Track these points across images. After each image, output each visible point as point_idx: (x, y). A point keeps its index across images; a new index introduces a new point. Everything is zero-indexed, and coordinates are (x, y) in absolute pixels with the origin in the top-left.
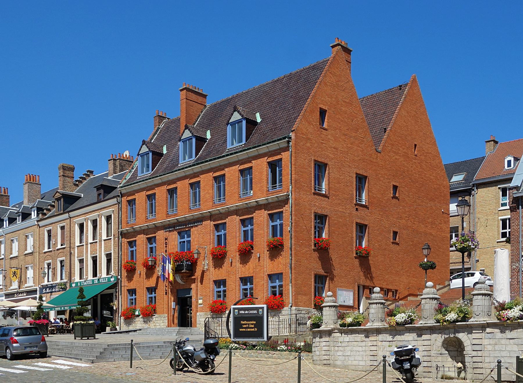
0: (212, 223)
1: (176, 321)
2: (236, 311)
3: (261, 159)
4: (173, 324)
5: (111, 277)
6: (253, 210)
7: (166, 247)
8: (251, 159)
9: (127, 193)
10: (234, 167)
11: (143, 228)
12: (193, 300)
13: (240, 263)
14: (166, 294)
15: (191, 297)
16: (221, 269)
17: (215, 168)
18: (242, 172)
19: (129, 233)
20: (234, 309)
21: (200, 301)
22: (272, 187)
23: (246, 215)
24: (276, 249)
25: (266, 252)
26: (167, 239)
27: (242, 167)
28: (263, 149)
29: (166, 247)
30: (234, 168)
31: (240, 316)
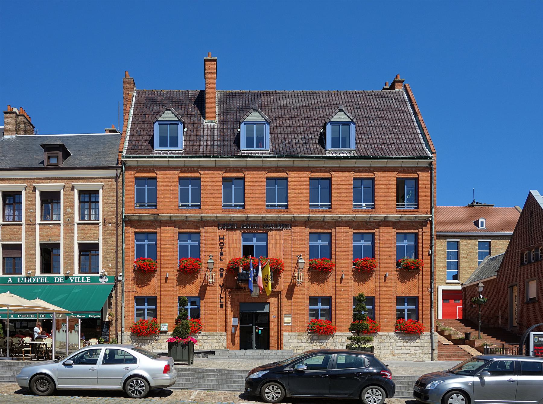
0: (308, 230)
1: (237, 341)
2: (536, 338)
3: (389, 173)
4: (233, 344)
5: (101, 277)
6: (374, 224)
7: (221, 248)
8: (373, 169)
9: (138, 167)
10: (347, 173)
11: (174, 219)
12: (273, 317)
13: (354, 281)
14: (221, 306)
15: (268, 314)
16: (322, 285)
17: (313, 168)
18: (225, 180)
19: (141, 221)
20: (535, 335)
21: (287, 319)
22: (397, 205)
23: (366, 228)
24: (363, 272)
25: (394, 272)
26: (223, 239)
27: (358, 175)
28: (397, 162)
29: (221, 248)
30: (346, 173)
31: (540, 343)
